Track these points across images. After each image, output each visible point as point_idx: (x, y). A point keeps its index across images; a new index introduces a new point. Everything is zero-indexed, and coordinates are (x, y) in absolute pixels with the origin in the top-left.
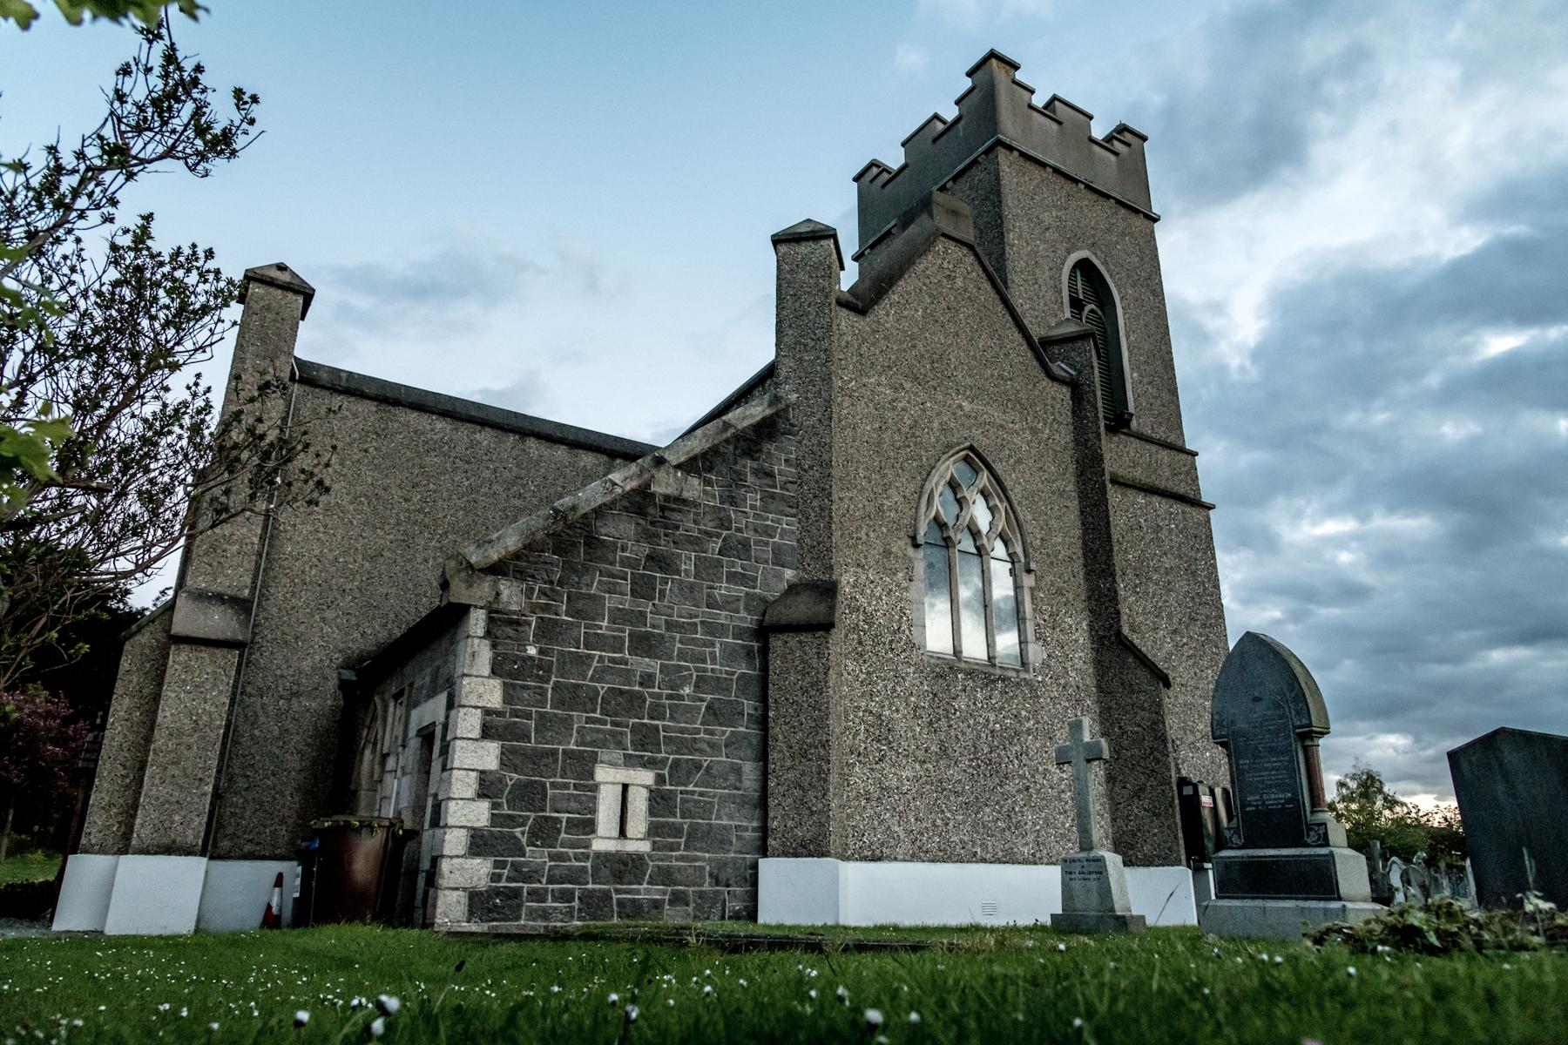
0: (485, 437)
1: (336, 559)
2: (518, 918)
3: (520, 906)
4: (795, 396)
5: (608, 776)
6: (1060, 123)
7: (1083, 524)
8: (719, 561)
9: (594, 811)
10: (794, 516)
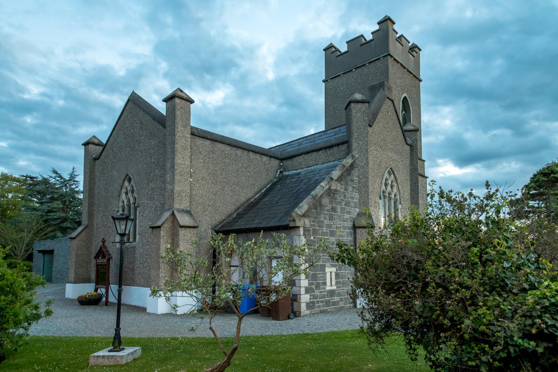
0: (239, 152)
1: (206, 196)
2: (315, 309)
3: (315, 305)
4: (357, 155)
5: (328, 270)
6: (402, 45)
7: (411, 189)
8: (345, 208)
9: (326, 280)
10: (358, 193)
